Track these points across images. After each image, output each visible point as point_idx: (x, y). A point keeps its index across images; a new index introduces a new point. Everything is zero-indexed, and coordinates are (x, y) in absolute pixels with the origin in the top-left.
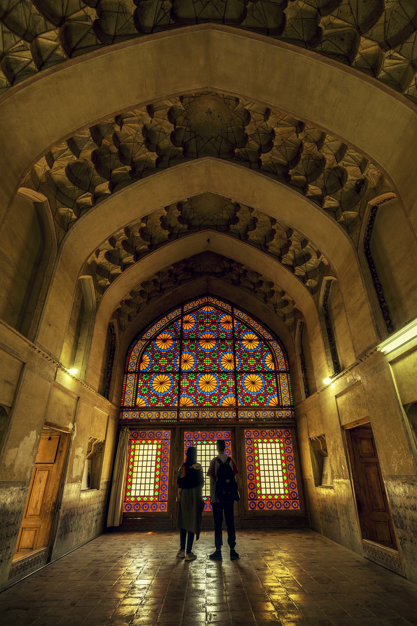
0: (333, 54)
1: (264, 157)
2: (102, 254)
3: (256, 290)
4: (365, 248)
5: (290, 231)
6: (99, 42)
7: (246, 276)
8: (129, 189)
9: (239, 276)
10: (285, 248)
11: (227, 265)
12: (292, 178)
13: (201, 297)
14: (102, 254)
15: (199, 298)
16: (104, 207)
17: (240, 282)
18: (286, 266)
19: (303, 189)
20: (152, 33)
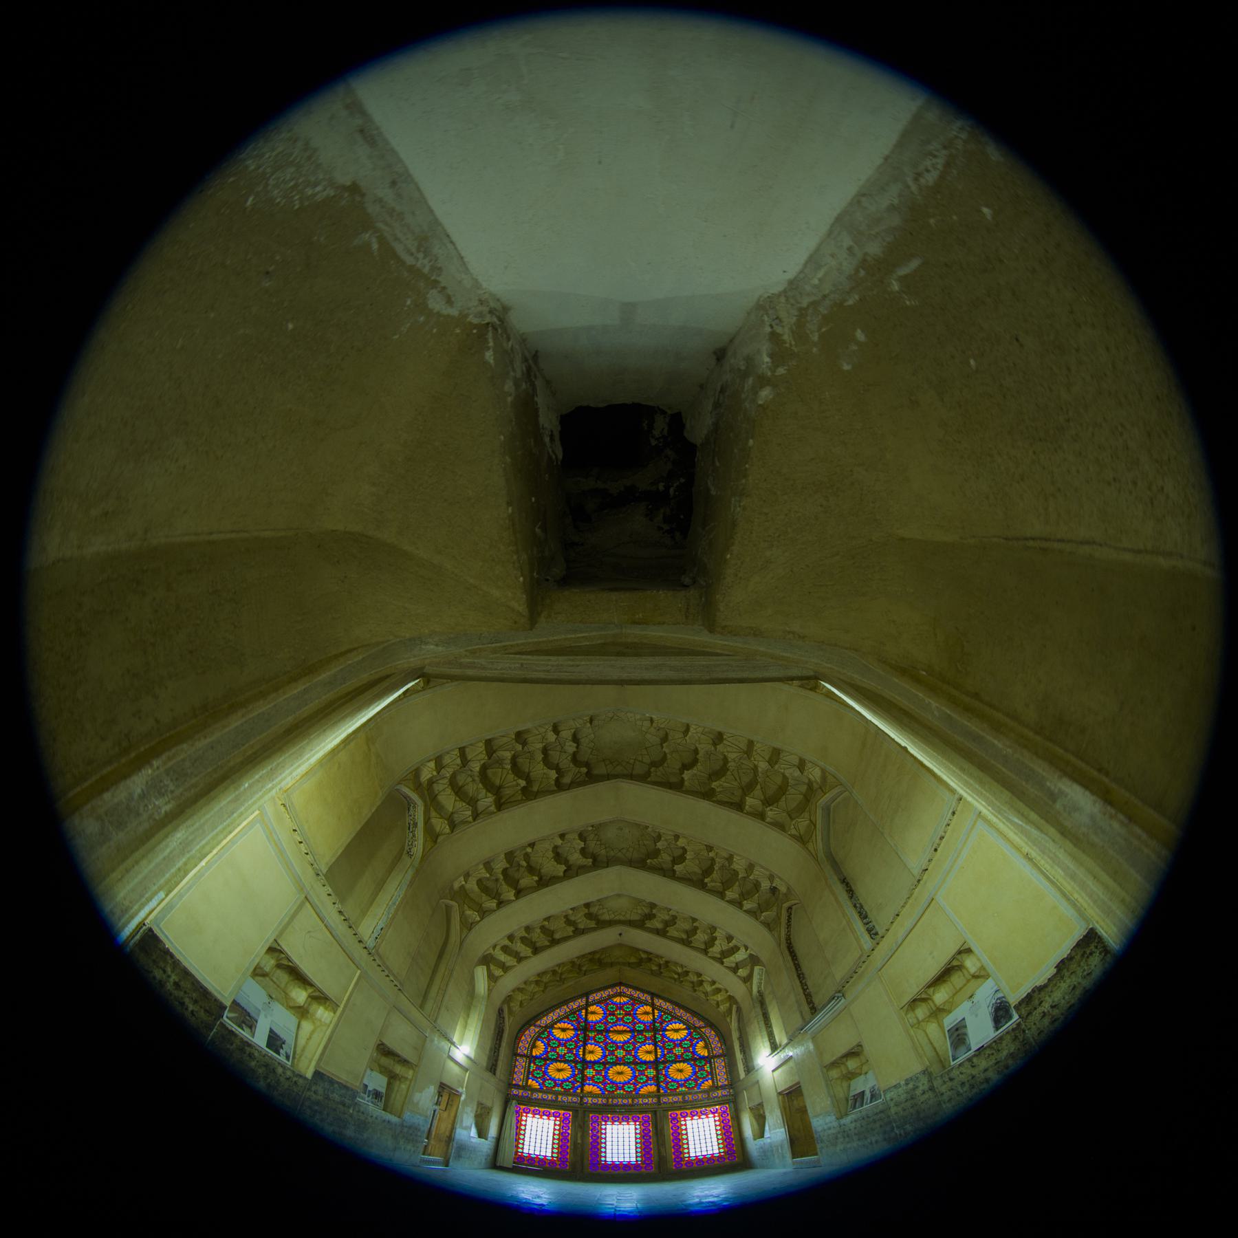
0: (727, 802)
1: (678, 868)
2: (498, 948)
3: (681, 979)
4: (787, 943)
5: (713, 929)
6: (524, 798)
7: (668, 966)
8: (534, 895)
9: (660, 966)
10: (711, 942)
11: (644, 956)
12: (708, 885)
13: (612, 986)
14: (498, 948)
15: (609, 988)
16: (504, 911)
17: (661, 973)
18: (714, 958)
19: (721, 895)
20: (568, 789)
